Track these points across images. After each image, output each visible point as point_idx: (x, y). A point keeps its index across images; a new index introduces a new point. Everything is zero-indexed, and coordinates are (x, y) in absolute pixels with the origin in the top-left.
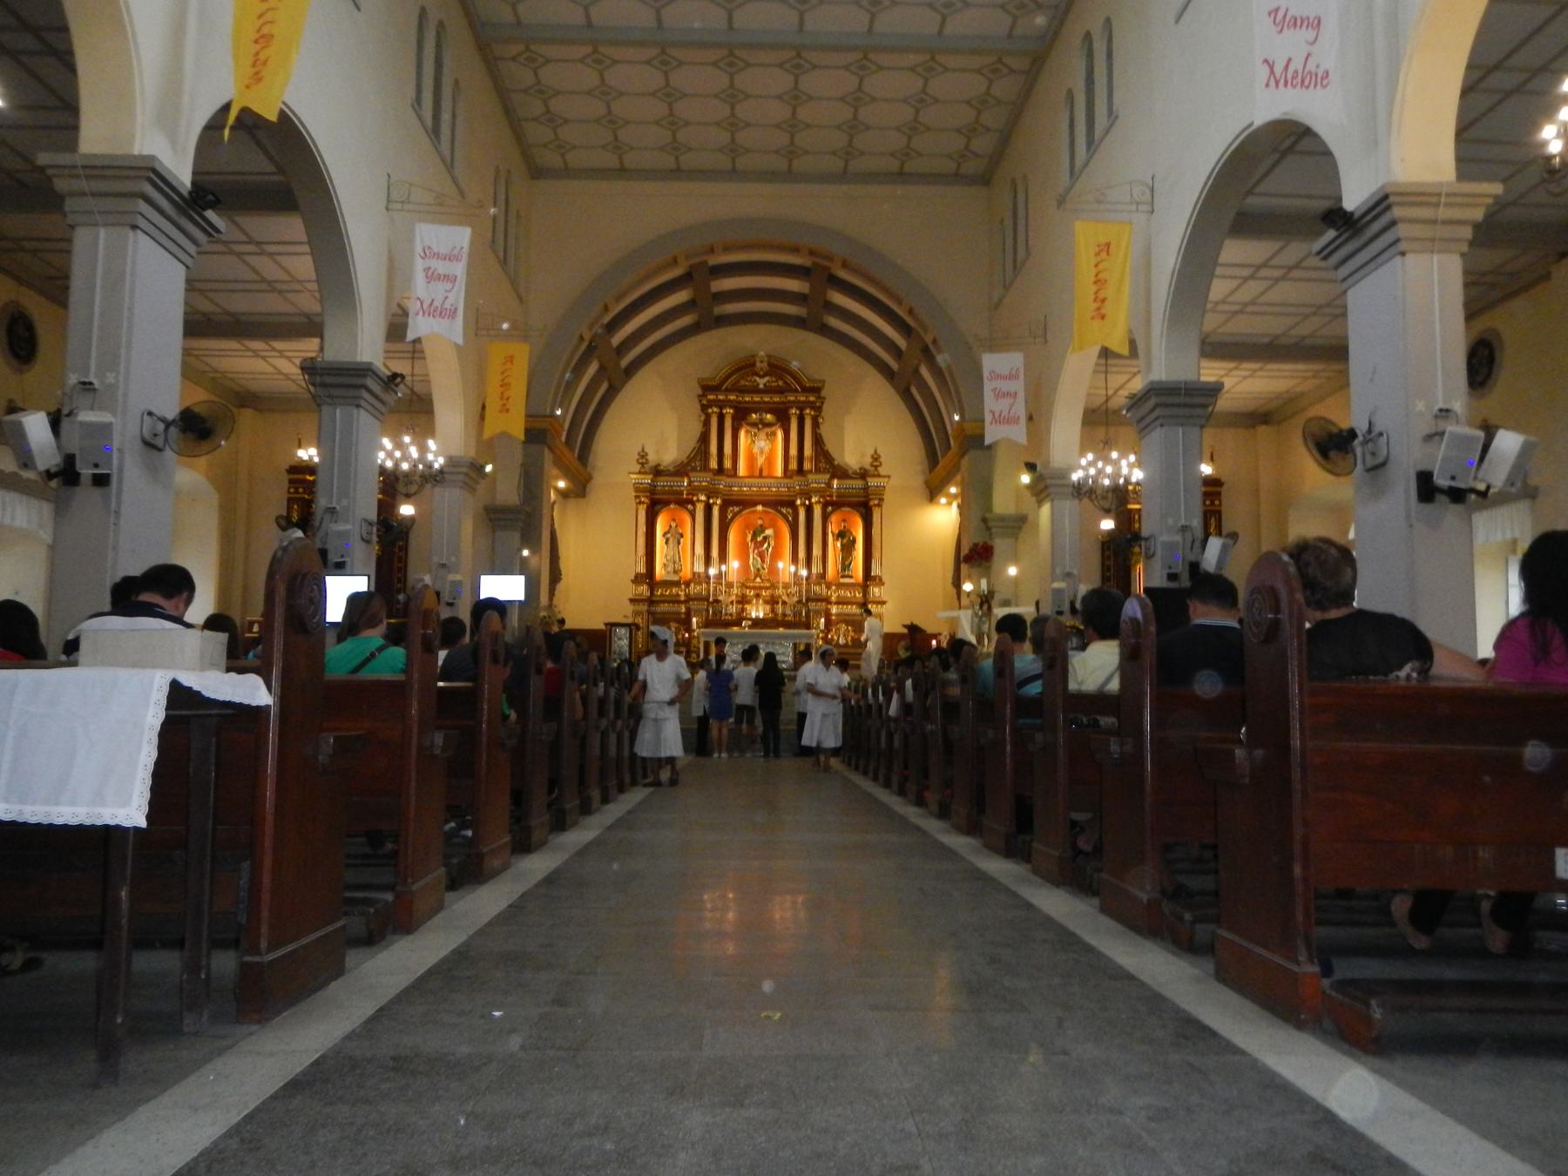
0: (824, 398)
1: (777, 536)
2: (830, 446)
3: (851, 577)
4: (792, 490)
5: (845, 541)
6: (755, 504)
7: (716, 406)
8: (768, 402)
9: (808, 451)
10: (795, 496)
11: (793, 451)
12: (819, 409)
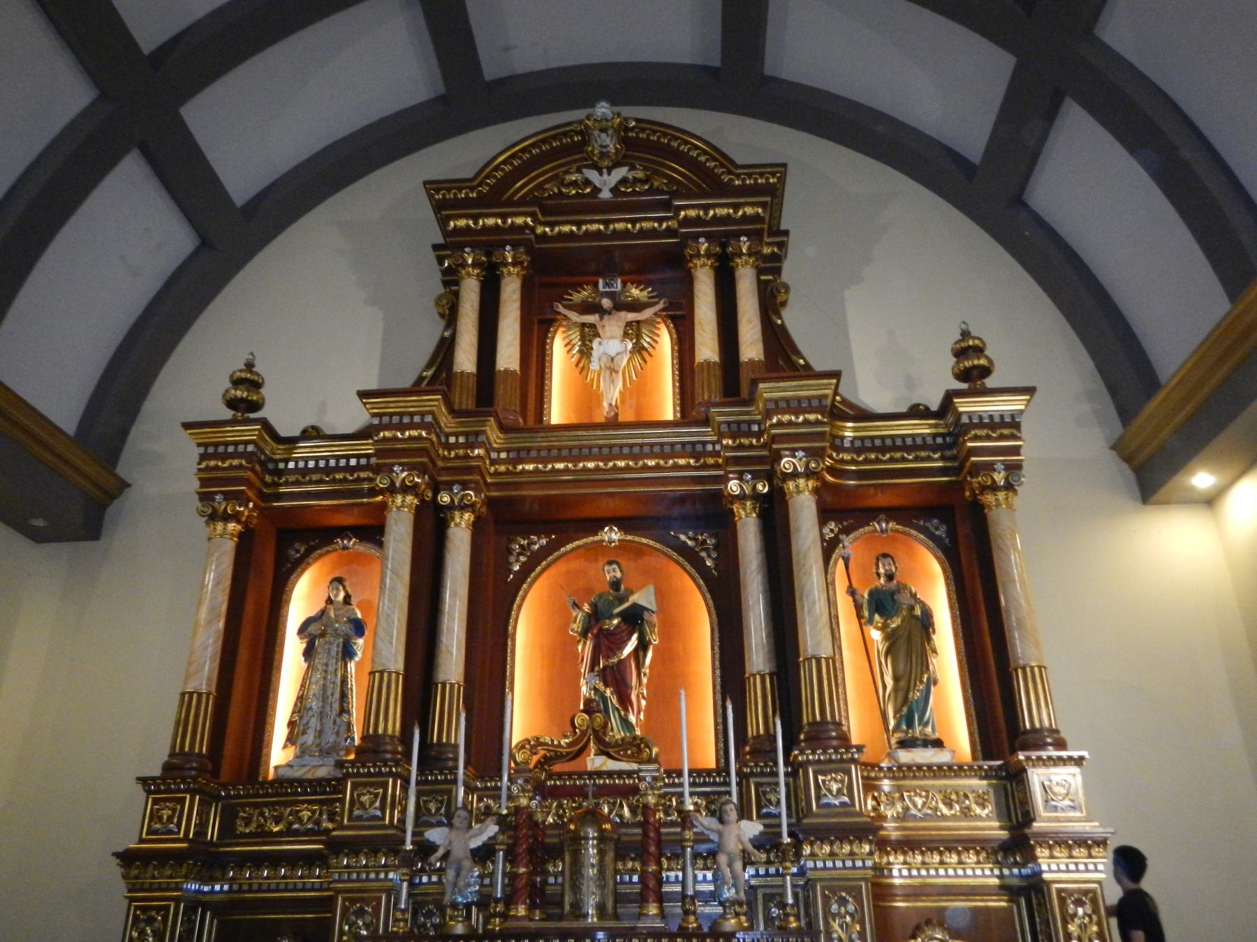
0: (786, 233)
1: (673, 629)
2: (813, 352)
3: (938, 744)
4: (711, 461)
5: (895, 623)
6: (595, 525)
7: (474, 246)
8: (626, 234)
9: (751, 347)
10: (724, 480)
11: (707, 349)
12: (770, 267)
